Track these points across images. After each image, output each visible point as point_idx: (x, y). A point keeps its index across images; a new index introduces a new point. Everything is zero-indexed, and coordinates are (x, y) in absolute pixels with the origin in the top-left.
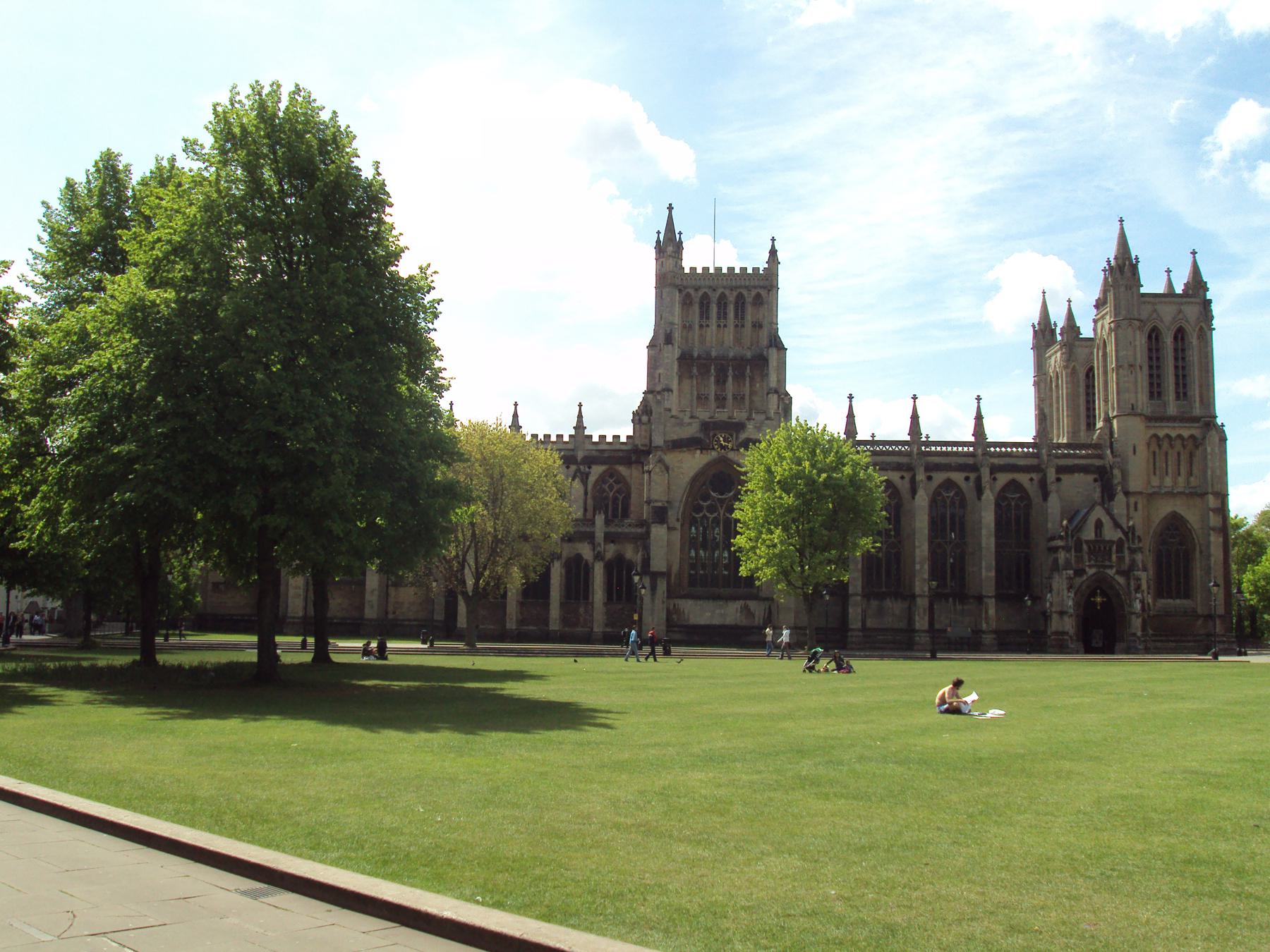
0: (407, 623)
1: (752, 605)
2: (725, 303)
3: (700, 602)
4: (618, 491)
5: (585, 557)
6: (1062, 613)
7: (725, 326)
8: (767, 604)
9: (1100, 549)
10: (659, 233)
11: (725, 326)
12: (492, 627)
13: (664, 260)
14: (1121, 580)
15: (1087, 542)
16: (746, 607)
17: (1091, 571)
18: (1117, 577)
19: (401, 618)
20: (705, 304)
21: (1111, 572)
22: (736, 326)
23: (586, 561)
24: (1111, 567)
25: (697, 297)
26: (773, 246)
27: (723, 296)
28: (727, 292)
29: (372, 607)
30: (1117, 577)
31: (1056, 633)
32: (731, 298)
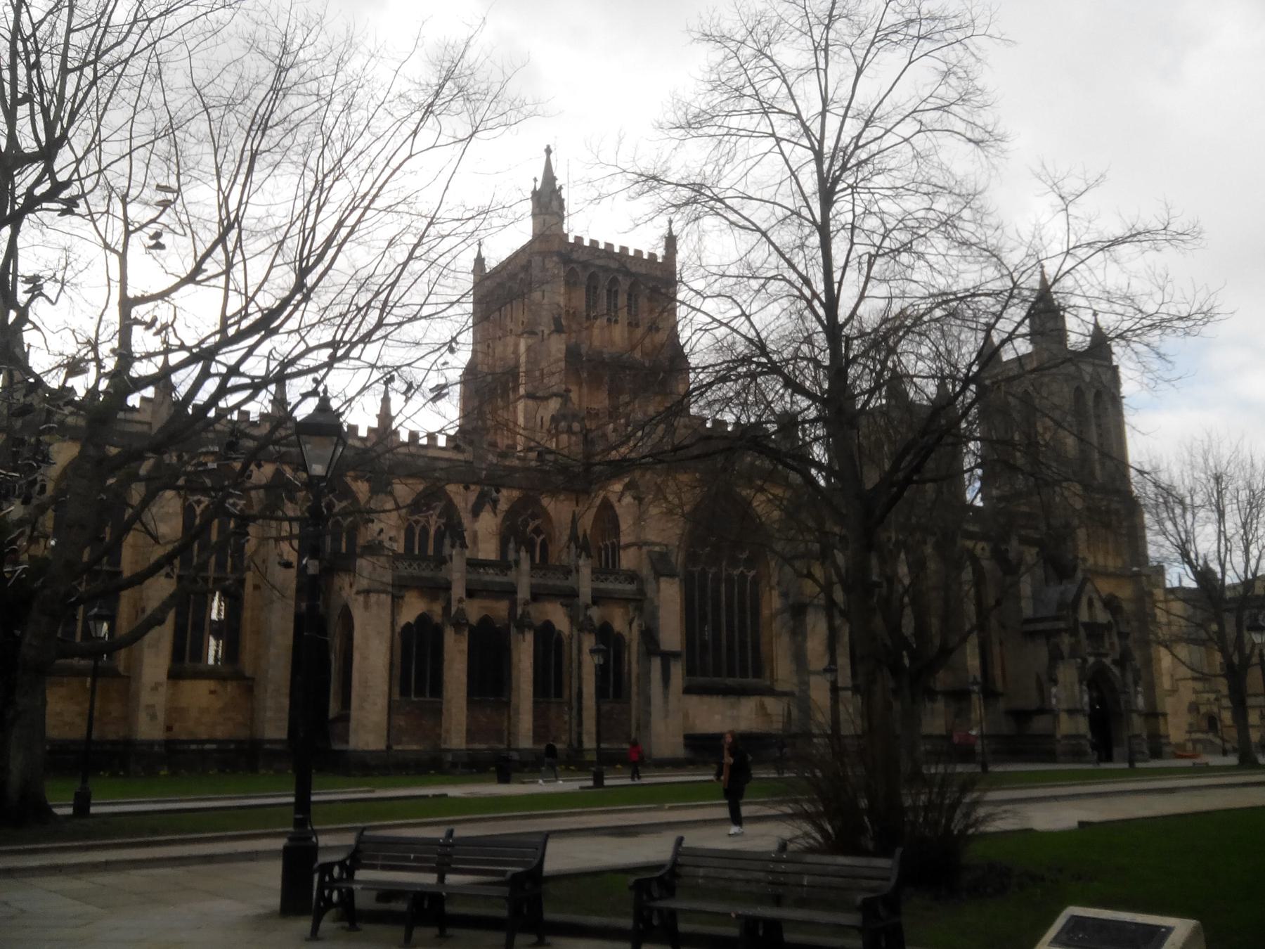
0: (193, 747)
1: (771, 703)
2: (616, 292)
3: (707, 699)
4: (537, 531)
5: (558, 627)
6: (1071, 712)
7: (616, 322)
8: (785, 700)
9: (1096, 632)
10: (535, 180)
11: (616, 322)
12: (415, 747)
13: (547, 217)
14: (1116, 671)
15: (1085, 625)
16: (762, 707)
17: (1091, 660)
18: (1112, 667)
19: (184, 737)
20: (592, 290)
21: (1107, 661)
22: (630, 324)
23: (560, 633)
24: (1106, 655)
25: (583, 277)
26: (670, 229)
27: (614, 281)
28: (620, 278)
29: (153, 717)
30: (1112, 667)
31: (1066, 737)
32: (624, 284)
